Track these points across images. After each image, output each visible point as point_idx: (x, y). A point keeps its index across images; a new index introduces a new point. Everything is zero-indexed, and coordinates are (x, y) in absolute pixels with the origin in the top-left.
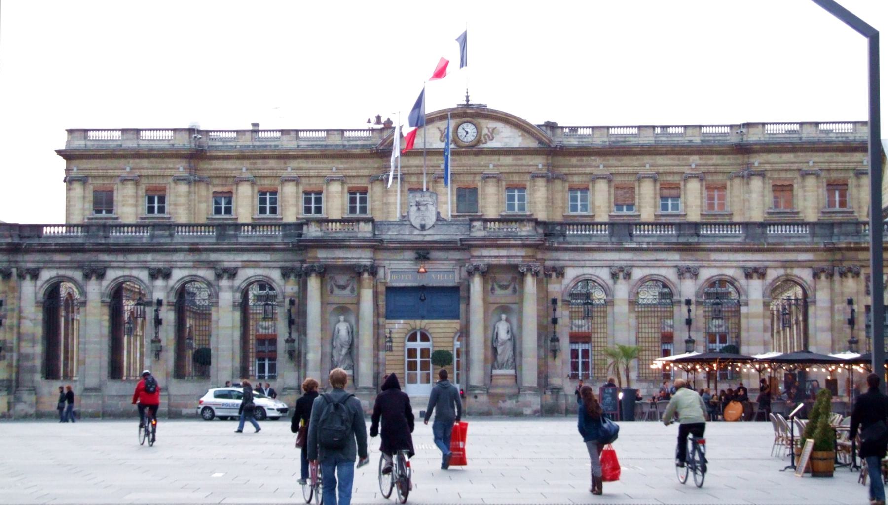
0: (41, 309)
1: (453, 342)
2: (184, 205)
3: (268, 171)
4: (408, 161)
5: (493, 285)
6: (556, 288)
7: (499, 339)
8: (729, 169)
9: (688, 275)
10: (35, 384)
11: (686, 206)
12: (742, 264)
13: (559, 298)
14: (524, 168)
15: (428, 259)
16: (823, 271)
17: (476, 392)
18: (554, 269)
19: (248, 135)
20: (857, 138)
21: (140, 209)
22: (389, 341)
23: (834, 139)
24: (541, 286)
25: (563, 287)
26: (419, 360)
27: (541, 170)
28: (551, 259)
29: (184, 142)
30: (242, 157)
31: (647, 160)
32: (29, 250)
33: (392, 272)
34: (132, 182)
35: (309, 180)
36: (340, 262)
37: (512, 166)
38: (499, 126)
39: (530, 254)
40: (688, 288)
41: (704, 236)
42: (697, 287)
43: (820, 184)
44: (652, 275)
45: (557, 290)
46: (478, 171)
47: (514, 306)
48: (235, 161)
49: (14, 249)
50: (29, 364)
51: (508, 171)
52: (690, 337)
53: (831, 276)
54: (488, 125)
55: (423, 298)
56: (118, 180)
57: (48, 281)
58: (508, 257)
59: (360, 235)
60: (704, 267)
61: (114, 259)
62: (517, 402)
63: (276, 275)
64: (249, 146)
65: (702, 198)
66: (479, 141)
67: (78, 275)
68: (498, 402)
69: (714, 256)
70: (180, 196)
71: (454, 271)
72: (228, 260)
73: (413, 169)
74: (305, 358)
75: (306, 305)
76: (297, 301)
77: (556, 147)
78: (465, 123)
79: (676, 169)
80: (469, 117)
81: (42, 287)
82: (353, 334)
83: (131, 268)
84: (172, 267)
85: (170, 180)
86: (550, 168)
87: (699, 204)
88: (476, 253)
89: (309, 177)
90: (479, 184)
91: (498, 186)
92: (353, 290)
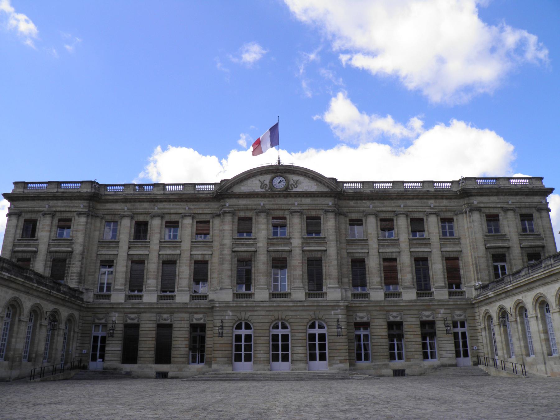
2: (82, 231)
3: (143, 210)
4: (238, 201)
8: (454, 209)
11: (429, 233)
14: (319, 206)
21: (53, 234)
22: (221, 329)
26: (243, 343)
27: (331, 206)
29: (86, 189)
30: (126, 200)
31: (402, 203)
34: (50, 216)
35: (170, 217)
37: (310, 204)
38: (301, 178)
43: (517, 217)
46: (287, 208)
48: (121, 204)
51: (307, 208)
54: (293, 178)
56: (41, 215)
65: (439, 228)
66: (287, 188)
70: (80, 225)
73: (241, 206)
77: (341, 191)
79: (420, 209)
80: (280, 173)
85: (75, 214)
86: (337, 206)
87: (437, 231)
89: (170, 214)
90: (288, 217)
91: (301, 218)
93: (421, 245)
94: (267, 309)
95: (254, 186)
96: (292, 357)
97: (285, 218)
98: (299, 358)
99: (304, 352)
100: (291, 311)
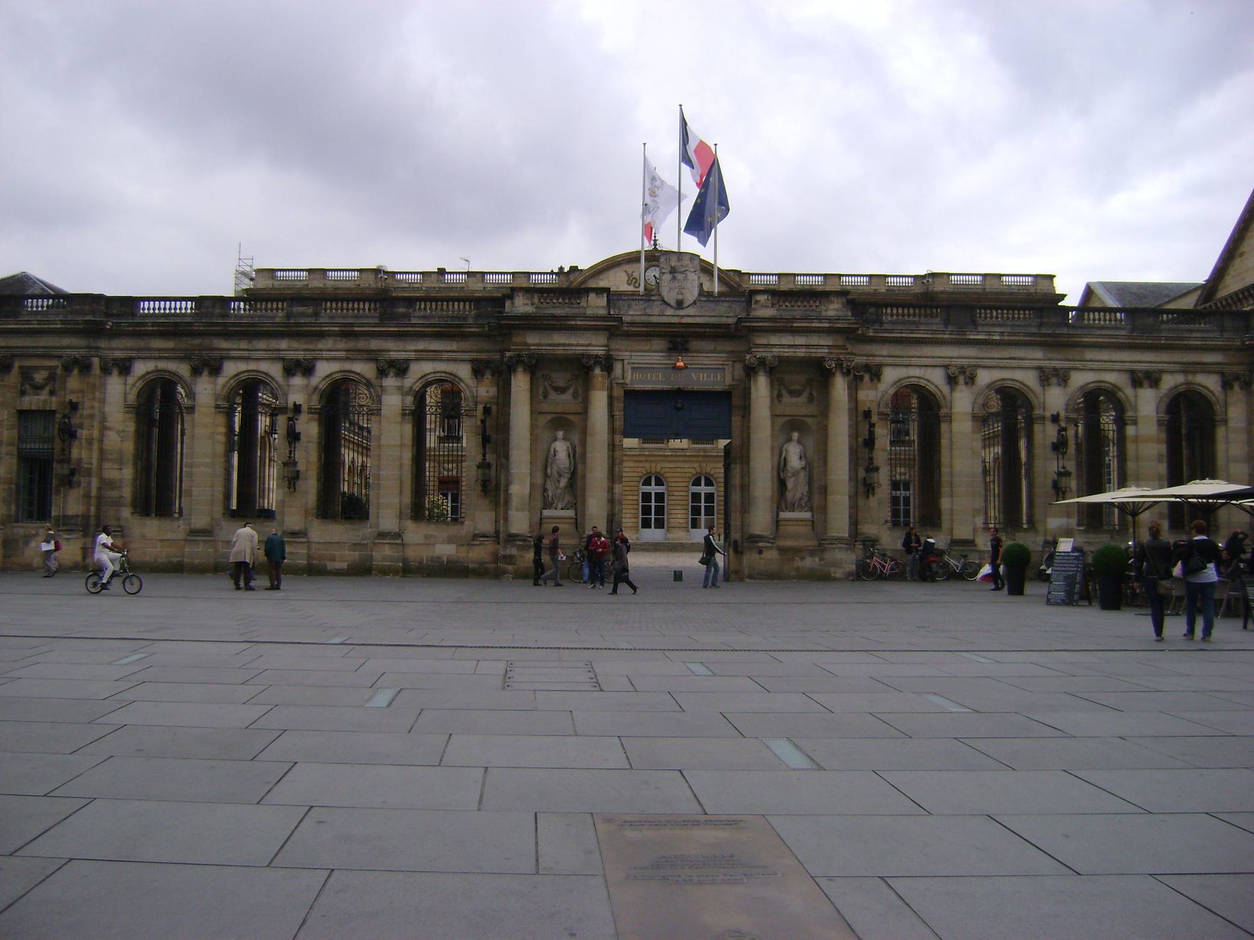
0: (133, 416)
1: (638, 486)
5: (780, 391)
6: (870, 396)
7: (788, 468)
9: (1054, 380)
10: (123, 523)
12: (1128, 366)
13: (874, 410)
15: (687, 350)
16: (1237, 378)
17: (760, 544)
18: (867, 368)
19: (434, 277)
20: (1038, 291)
23: (1015, 291)
24: (853, 389)
25: (879, 395)
28: (862, 355)
32: (116, 334)
33: (633, 368)
36: (560, 351)
39: (840, 343)
40: (1055, 399)
42: (1067, 398)
44: (1003, 379)
45: (871, 398)
47: (809, 420)
49: (94, 331)
50: (115, 494)
55: (679, 405)
57: (143, 376)
58: (807, 346)
59: (589, 312)
60: (1077, 369)
61: (235, 346)
62: (821, 559)
64: (435, 288)
67: (183, 369)
68: (793, 559)
69: (1090, 354)
71: (724, 369)
72: (395, 350)
74: (507, 490)
75: (509, 414)
76: (494, 408)
78: (652, 266)
81: (134, 385)
82: (578, 457)
83: (258, 359)
84: (315, 359)
92: (575, 396)
94: (636, 459)
96: (669, 523)
98: (678, 525)
99: (683, 516)
100: (670, 461)
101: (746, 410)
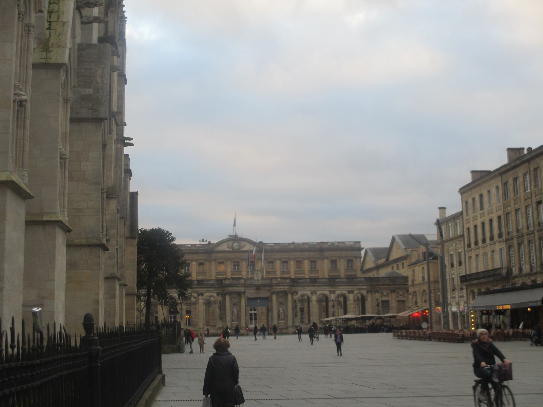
6: (296, 297)
9: (332, 293)
18: (295, 292)
28: (294, 289)
36: (235, 291)
41: (337, 282)
52: (334, 310)
53: (371, 292)
54: (243, 243)
58: (283, 288)
63: (215, 295)
66: (240, 248)
76: (221, 302)
82: (239, 311)
88: (274, 288)
92: (238, 299)
93: (300, 274)
95: (224, 247)
97: (239, 262)
101: (271, 301)
